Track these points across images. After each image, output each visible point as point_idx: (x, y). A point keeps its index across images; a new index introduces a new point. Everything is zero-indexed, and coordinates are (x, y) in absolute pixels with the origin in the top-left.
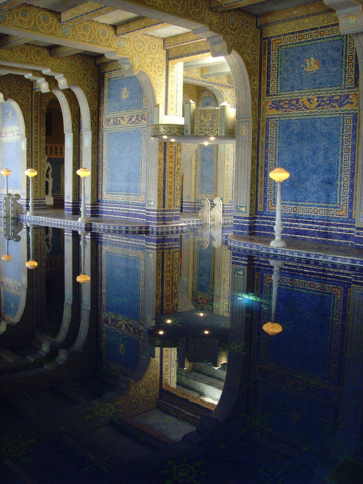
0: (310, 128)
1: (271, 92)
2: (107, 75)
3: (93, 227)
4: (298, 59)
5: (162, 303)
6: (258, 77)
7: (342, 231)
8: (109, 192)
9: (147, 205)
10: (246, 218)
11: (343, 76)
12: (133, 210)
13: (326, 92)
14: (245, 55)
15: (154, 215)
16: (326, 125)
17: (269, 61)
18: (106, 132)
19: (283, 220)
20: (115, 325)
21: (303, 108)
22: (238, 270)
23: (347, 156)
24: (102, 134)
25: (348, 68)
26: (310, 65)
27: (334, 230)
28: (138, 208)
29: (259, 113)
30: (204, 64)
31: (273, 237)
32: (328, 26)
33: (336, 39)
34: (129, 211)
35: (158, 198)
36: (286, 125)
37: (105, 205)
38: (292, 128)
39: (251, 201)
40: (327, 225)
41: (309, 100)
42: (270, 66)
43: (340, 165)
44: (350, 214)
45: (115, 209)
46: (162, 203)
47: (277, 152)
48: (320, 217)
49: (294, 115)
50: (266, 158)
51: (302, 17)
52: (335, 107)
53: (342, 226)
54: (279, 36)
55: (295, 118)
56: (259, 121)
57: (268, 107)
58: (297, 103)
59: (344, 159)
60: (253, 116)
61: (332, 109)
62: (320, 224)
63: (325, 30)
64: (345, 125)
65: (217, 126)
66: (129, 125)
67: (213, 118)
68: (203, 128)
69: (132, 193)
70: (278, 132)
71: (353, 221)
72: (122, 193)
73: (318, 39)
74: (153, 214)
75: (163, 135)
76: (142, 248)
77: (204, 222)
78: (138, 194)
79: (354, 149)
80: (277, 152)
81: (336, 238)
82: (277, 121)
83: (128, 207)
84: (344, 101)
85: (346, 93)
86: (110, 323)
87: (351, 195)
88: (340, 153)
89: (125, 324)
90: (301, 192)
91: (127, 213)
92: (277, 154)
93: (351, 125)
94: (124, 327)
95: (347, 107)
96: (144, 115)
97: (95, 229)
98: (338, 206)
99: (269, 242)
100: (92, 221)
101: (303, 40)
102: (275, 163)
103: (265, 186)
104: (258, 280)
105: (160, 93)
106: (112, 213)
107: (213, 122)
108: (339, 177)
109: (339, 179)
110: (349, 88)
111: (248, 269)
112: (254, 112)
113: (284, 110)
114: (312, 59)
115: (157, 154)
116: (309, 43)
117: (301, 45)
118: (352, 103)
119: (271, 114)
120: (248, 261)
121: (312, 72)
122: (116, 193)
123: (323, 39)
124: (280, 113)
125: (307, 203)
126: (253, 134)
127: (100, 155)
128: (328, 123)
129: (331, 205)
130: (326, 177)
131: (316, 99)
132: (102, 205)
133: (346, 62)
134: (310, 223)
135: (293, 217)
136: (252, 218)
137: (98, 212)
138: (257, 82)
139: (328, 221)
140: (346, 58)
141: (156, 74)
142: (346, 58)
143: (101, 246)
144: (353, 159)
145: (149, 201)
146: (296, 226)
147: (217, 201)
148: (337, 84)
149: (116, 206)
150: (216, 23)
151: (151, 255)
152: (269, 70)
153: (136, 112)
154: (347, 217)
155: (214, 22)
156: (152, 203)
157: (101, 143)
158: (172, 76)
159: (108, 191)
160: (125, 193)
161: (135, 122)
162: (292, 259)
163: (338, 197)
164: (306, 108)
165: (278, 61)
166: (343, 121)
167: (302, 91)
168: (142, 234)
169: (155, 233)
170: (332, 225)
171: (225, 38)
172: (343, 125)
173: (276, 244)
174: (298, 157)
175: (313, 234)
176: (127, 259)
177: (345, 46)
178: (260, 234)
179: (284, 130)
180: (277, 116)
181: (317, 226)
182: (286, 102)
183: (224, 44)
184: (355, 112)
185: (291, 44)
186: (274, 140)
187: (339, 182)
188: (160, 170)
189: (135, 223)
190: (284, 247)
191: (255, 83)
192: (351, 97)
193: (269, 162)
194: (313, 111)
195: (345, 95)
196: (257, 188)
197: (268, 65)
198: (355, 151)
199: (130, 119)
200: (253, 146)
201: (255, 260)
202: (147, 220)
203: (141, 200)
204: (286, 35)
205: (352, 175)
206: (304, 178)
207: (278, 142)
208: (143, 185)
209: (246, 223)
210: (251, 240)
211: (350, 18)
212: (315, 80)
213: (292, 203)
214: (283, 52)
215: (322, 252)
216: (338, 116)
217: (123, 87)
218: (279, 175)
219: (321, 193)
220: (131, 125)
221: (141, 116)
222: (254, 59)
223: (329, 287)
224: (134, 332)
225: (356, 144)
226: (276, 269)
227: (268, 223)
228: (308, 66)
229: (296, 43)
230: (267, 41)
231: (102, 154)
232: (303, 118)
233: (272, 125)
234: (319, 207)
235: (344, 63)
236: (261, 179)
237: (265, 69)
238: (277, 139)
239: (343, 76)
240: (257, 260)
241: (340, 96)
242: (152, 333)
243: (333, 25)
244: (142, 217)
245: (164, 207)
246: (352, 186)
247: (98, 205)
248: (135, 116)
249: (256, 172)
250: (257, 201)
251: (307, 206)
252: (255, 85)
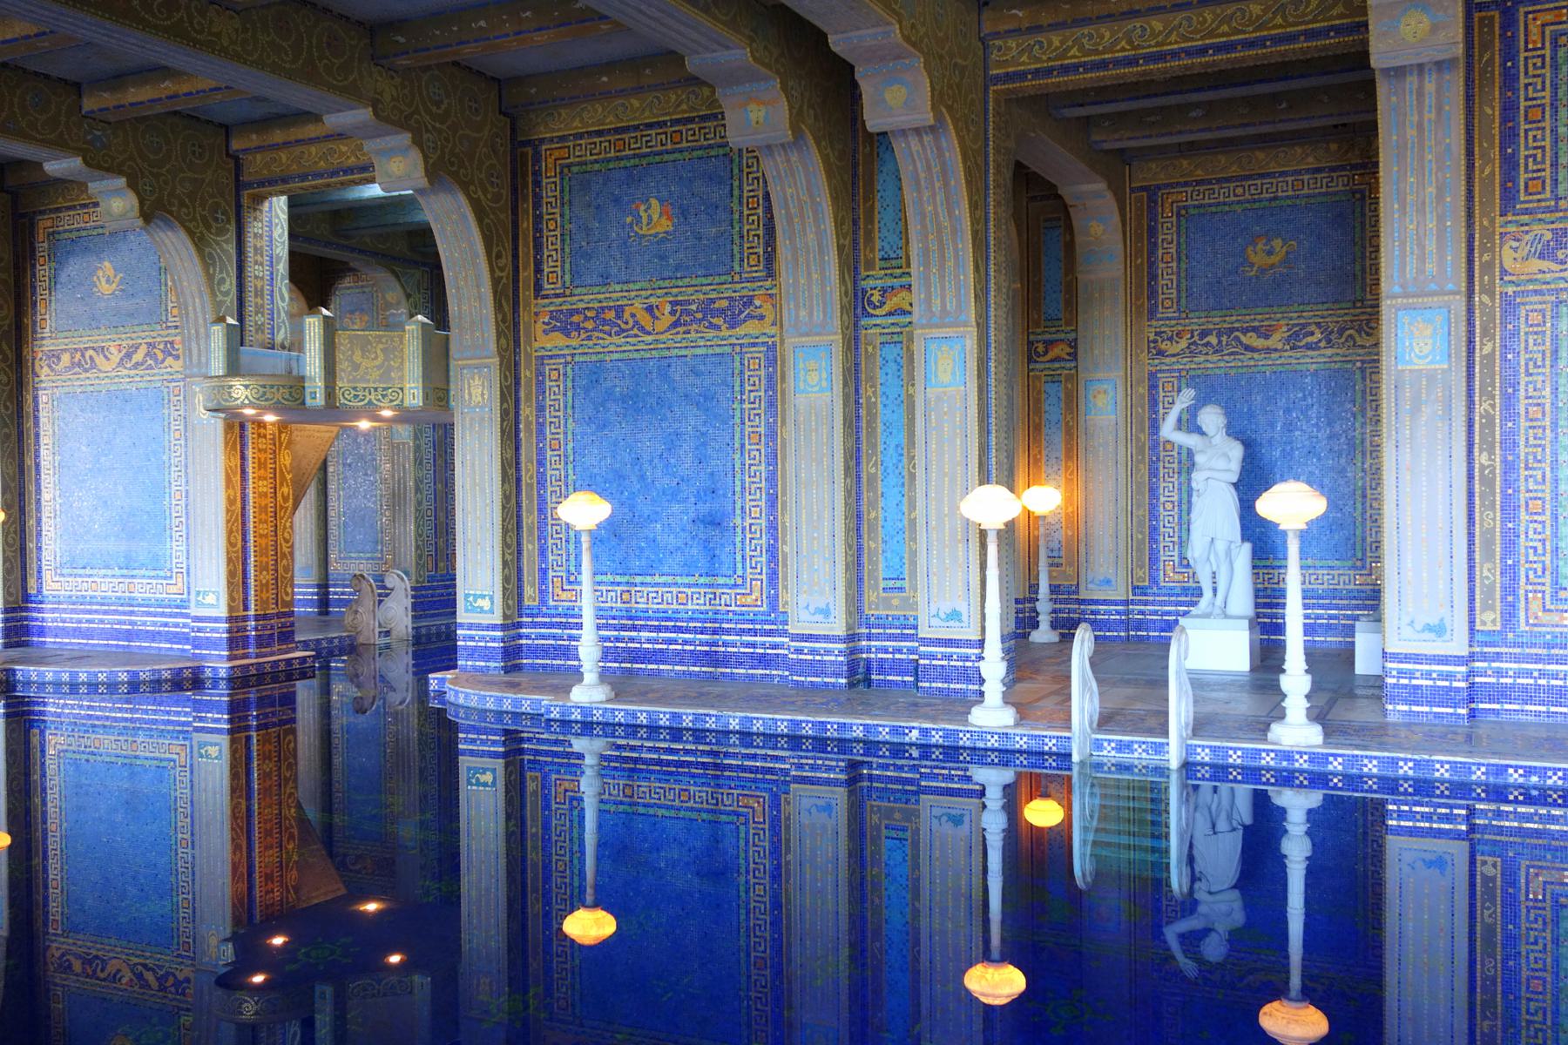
0: (657, 382)
1: (546, 286)
2: (44, 224)
3: (19, 676)
4: (617, 200)
5: (250, 888)
6: (509, 245)
7: (754, 645)
8: (65, 571)
9: (192, 604)
10: (494, 627)
11: (736, 249)
12: (149, 623)
13: (694, 292)
14: (472, 188)
15: (220, 631)
16: (697, 374)
17: (537, 205)
19: (599, 628)
20: (94, 972)
21: (635, 331)
22: (477, 770)
23: (756, 454)
24: (36, 398)
25: (746, 227)
26: (650, 217)
27: (734, 643)
28: (163, 615)
29: (517, 343)
30: (348, 201)
31: (577, 675)
32: (691, 120)
33: (713, 153)
34: (132, 623)
35: (230, 584)
36: (595, 373)
37: (53, 611)
38: (609, 384)
39: (506, 580)
40: (715, 632)
41: (650, 309)
42: (540, 217)
43: (738, 476)
44: (773, 602)
45: (88, 621)
46: (239, 596)
47: (570, 445)
48: (694, 612)
49: (612, 348)
50: (541, 463)
51: (621, 93)
52: (718, 328)
53: (755, 633)
54: (562, 138)
55: (616, 356)
56: (517, 364)
57: (540, 327)
58: (618, 317)
59: (748, 462)
60: (501, 352)
61: (711, 334)
62: (695, 631)
63: (683, 128)
64: (747, 373)
65: (402, 378)
66: (126, 372)
67: (386, 359)
68: (360, 385)
69: (143, 572)
70: (570, 394)
71: (781, 618)
72: (109, 572)
73: (668, 152)
74: (213, 630)
75: (243, 406)
76: (184, 733)
77: (361, 640)
78: (161, 573)
79: (772, 434)
80: (570, 445)
81: (740, 664)
82: (566, 363)
83: (131, 613)
84: (741, 312)
85: (745, 292)
86: (77, 966)
87: (772, 552)
88: (737, 445)
89: (132, 968)
90: (642, 549)
91: (128, 631)
92: (570, 452)
93: (762, 373)
94: (127, 976)
95: (751, 328)
96: (172, 343)
97: (28, 683)
98: (740, 581)
99: (567, 690)
100: (13, 662)
101: (628, 152)
102: (566, 477)
103: (542, 537)
104: (535, 793)
105: (222, 281)
106: (77, 632)
107: (390, 369)
108: (738, 506)
109: (738, 512)
110: (753, 280)
111: (507, 766)
112: (503, 341)
113: (583, 336)
114: (654, 202)
115: (221, 458)
116: (644, 162)
117: (622, 164)
118: (762, 318)
119: (549, 346)
120: (504, 744)
121: (656, 235)
122: (88, 571)
123: (681, 151)
124: (574, 343)
125: (657, 579)
126: (503, 399)
127: (29, 462)
128: (702, 368)
129: (721, 580)
130: (704, 508)
131: (668, 308)
132: (40, 611)
133: (741, 213)
134: (667, 629)
135: (622, 618)
136: (511, 626)
137: (27, 631)
138: (506, 260)
139: (715, 621)
140: (740, 203)
141: (208, 228)
142: (740, 203)
143: (42, 732)
144: (772, 459)
145: (198, 593)
146: (632, 640)
147: (391, 580)
148: (722, 269)
149: (90, 612)
150: (393, 99)
151: (213, 751)
152: (538, 230)
153: (144, 336)
154: (764, 608)
155: (387, 97)
156: (210, 599)
157: (31, 423)
158: (255, 235)
162: (632, 729)
163: (739, 558)
164: (642, 329)
165: (563, 204)
166: (742, 364)
167: (631, 286)
168: (182, 689)
169: (223, 684)
170: (728, 632)
171: (418, 142)
172: (742, 372)
174: (627, 458)
175: (680, 658)
176: (131, 767)
177: (736, 171)
178: (533, 667)
179: (587, 390)
180: (566, 352)
181: (687, 636)
182: (589, 314)
183: (415, 156)
184: (770, 341)
185: (596, 161)
186: (561, 414)
187: (738, 521)
188: (231, 502)
189: (160, 657)
190: (609, 701)
191: (502, 262)
192: (757, 303)
193: (549, 473)
194: (663, 337)
195: (742, 297)
196: (519, 544)
197: (535, 215)
198: (774, 440)
199: (129, 356)
200: (503, 432)
201: (522, 740)
202: (195, 647)
204: (580, 136)
205: (772, 501)
206: (647, 513)
207: (570, 420)
208: (177, 548)
209: (493, 640)
210: (514, 686)
211: (753, 107)
212: (662, 258)
213: (618, 579)
214: (573, 182)
215: (712, 707)
216: (728, 349)
217: (101, 260)
218: (583, 511)
219: (695, 551)
220: (132, 372)
222: (497, 198)
223: (731, 799)
224: (162, 989)
225: (775, 422)
226: (589, 760)
227: (554, 637)
228: (645, 221)
229: (609, 160)
230: (529, 150)
231: (37, 456)
232: (636, 355)
233: (554, 375)
234: (689, 586)
235: (736, 216)
236: (530, 519)
237: (526, 224)
238: (569, 411)
239: (736, 249)
240: (529, 740)
241: (730, 299)
242: (230, 981)
243: (704, 118)
244: (185, 639)
245: (246, 608)
246: (773, 527)
247: (27, 609)
249: (514, 501)
250: (520, 579)
251: (657, 584)
252: (502, 270)
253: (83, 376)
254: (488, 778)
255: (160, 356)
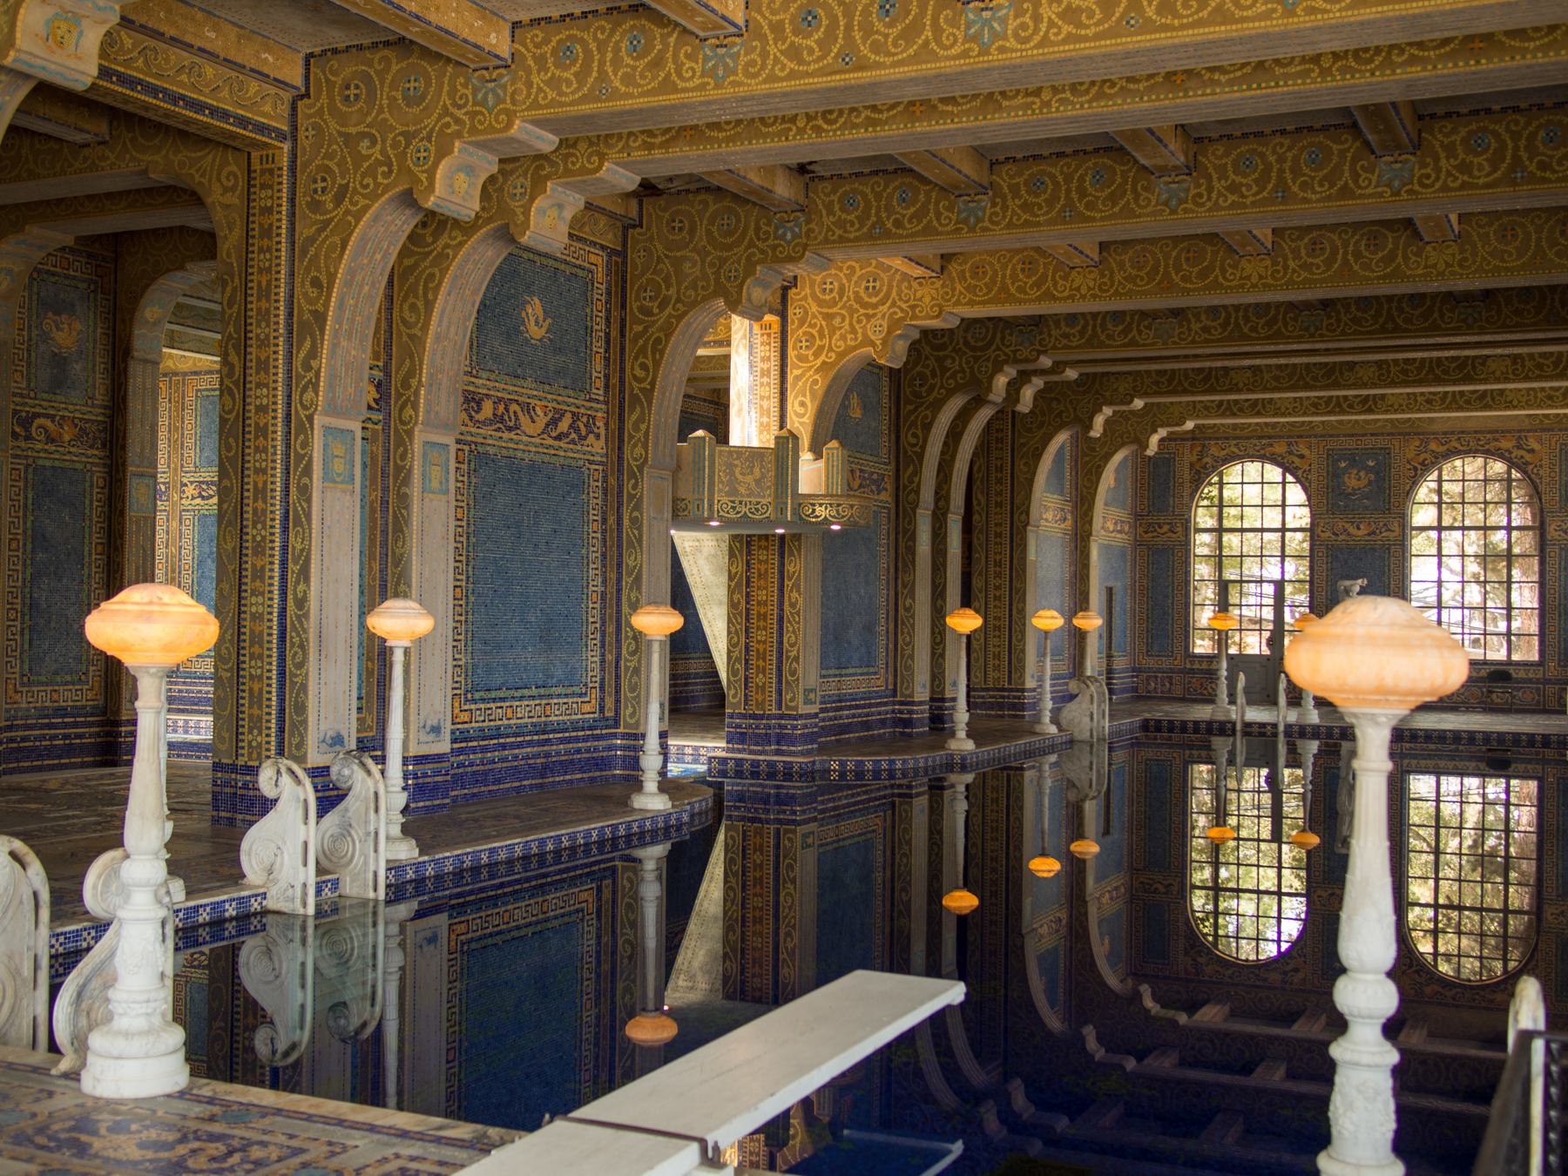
8: (477, 695)
18: (466, 448)
34: (548, 755)
66: (550, 442)
69: (559, 690)
72: (526, 692)
78: (576, 689)
125: (851, 671)
149: (504, 747)
159: (475, 689)
160: (534, 692)
161: (567, 435)
173: (962, 744)
199: (554, 422)
203: (587, 708)
220: (556, 443)
221: (585, 419)
248: (568, 415)
253: (506, 435)
254: (810, 841)
255: (583, 431)
